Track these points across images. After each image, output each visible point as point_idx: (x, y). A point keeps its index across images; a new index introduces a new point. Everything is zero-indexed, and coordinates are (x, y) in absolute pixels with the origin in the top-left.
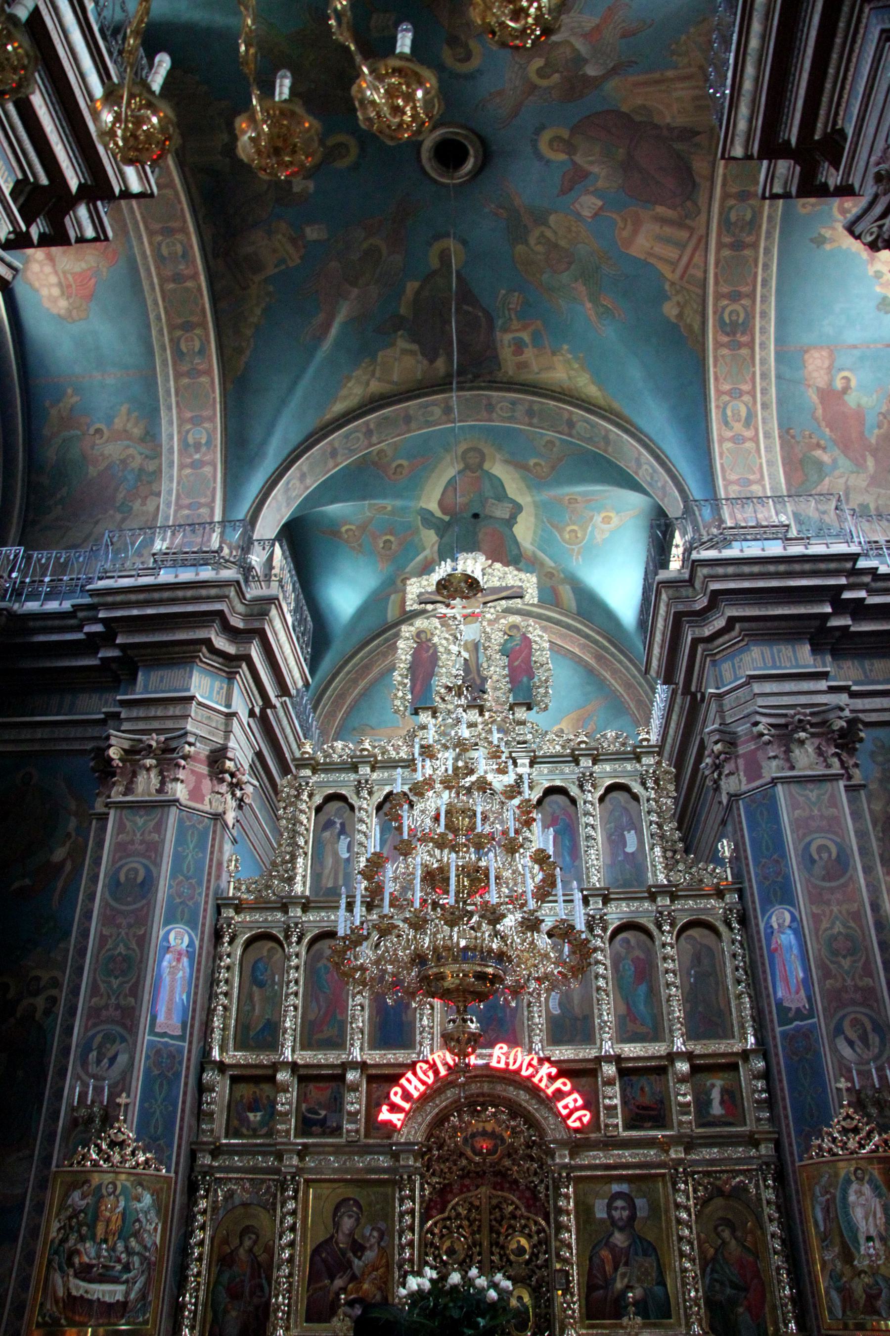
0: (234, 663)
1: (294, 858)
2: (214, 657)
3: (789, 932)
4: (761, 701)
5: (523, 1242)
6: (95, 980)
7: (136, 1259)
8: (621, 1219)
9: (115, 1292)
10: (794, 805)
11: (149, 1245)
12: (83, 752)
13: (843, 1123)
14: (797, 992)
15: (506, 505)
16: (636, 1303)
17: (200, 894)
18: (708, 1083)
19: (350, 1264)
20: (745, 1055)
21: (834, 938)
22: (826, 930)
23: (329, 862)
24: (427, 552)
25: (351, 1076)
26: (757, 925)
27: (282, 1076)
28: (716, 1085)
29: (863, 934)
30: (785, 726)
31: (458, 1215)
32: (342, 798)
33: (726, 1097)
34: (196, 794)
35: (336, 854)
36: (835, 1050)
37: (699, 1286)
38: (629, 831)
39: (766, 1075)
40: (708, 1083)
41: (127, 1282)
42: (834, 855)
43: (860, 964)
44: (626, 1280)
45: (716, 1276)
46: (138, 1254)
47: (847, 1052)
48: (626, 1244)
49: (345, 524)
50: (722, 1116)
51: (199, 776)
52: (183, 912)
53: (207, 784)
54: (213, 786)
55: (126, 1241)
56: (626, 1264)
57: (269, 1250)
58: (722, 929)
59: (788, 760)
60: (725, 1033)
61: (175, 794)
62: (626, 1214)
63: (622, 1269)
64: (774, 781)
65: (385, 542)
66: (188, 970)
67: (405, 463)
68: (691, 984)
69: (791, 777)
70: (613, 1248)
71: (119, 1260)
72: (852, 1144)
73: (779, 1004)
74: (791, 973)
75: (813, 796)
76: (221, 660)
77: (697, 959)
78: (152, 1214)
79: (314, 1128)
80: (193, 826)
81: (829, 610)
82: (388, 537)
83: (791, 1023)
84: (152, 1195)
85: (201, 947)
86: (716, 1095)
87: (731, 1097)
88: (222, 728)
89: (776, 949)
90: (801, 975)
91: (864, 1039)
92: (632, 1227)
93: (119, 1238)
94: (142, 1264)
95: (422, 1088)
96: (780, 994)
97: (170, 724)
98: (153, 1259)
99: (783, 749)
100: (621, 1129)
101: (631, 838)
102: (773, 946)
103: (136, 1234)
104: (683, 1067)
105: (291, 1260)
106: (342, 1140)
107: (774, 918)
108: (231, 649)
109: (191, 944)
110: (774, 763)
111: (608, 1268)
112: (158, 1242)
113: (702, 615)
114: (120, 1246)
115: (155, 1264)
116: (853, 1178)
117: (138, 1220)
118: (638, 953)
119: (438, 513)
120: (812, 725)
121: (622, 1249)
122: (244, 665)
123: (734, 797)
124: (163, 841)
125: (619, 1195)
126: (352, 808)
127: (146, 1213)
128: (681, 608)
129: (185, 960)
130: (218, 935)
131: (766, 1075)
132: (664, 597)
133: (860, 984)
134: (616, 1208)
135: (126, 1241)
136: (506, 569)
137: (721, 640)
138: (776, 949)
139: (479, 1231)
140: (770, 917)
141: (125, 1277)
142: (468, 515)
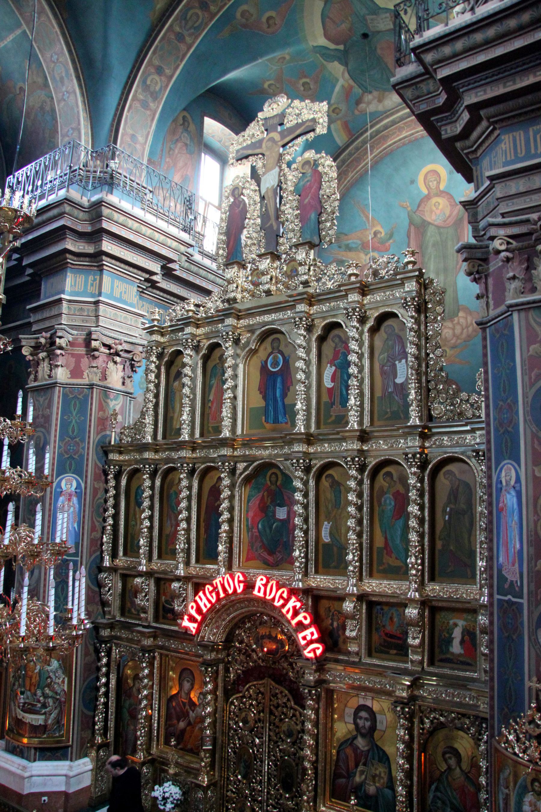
0: (98, 259)
2: (82, 259)
6: (24, 518)
7: (50, 701)
8: (364, 727)
9: (38, 719)
11: (59, 692)
15: (384, 16)
17: (83, 448)
18: (451, 622)
19: (188, 713)
24: (341, 82)
33: (466, 637)
38: (400, 362)
40: (451, 622)
41: (45, 714)
44: (363, 777)
45: (439, 794)
46: (51, 697)
48: (366, 748)
49: (264, 82)
50: (460, 655)
52: (71, 465)
54: (90, 362)
55: (43, 689)
56: (365, 764)
61: (56, 378)
62: (368, 724)
63: (361, 768)
65: (304, 84)
66: (77, 506)
67: (273, 14)
68: (445, 521)
69: (528, 303)
71: (39, 701)
76: (87, 259)
78: (60, 672)
79: (169, 615)
80: (75, 397)
82: (304, 80)
83: (506, 596)
84: (58, 661)
85: (86, 488)
88: (93, 314)
92: (372, 736)
93: (38, 688)
94: (54, 703)
95: (209, 605)
96: (501, 559)
97: (47, 324)
98: (63, 699)
99: (524, 266)
102: (501, 505)
103: (49, 686)
108: (90, 249)
109: (79, 486)
110: (514, 285)
111: (352, 764)
112: (66, 689)
114: (39, 692)
115: (65, 702)
117: (50, 677)
119: (332, 46)
121: (362, 751)
122: (104, 258)
124: (52, 414)
127: (55, 673)
129: (75, 499)
134: (361, 718)
135: (43, 689)
136: (303, 104)
139: (263, 711)
141: (43, 711)
142: (357, 37)
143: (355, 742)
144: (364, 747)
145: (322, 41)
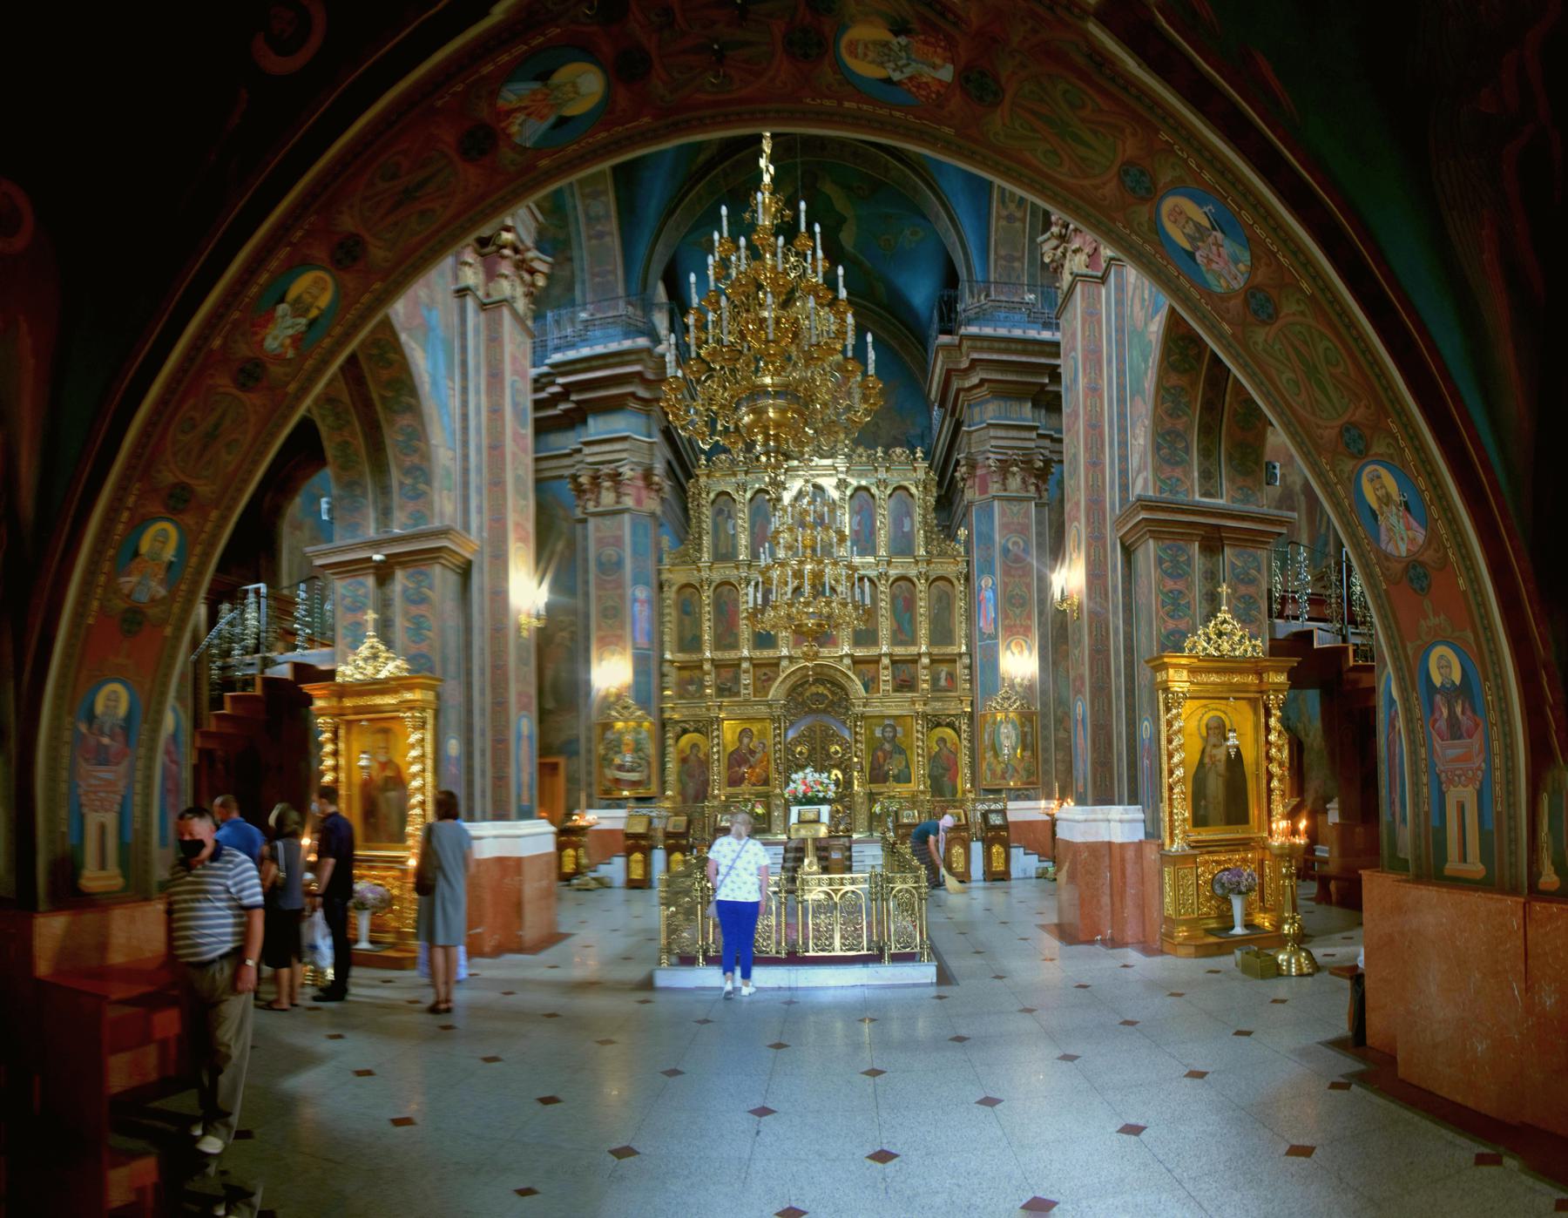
1: (700, 538)
4: (994, 443)
10: (1003, 514)
12: (561, 477)
16: (894, 776)
19: (749, 761)
20: (960, 655)
23: (722, 536)
25: (745, 665)
27: (707, 667)
28: (944, 670)
30: (1006, 461)
32: (728, 494)
34: (639, 501)
35: (726, 532)
37: (927, 768)
39: (970, 667)
51: (638, 488)
53: (644, 493)
57: (707, 755)
58: (956, 582)
59: (1004, 484)
60: (952, 643)
64: (994, 497)
70: (884, 751)
72: (1006, 705)
73: (980, 629)
75: (1015, 509)
77: (940, 599)
81: (1047, 381)
86: (943, 675)
87: (951, 677)
101: (907, 522)
104: (925, 661)
105: (718, 760)
106: (741, 699)
111: (881, 760)
113: (966, 372)
118: (906, 594)
120: (1022, 462)
123: (971, 503)
126: (734, 500)
128: (951, 366)
130: (661, 586)
131: (970, 667)
132: (940, 355)
137: (975, 391)
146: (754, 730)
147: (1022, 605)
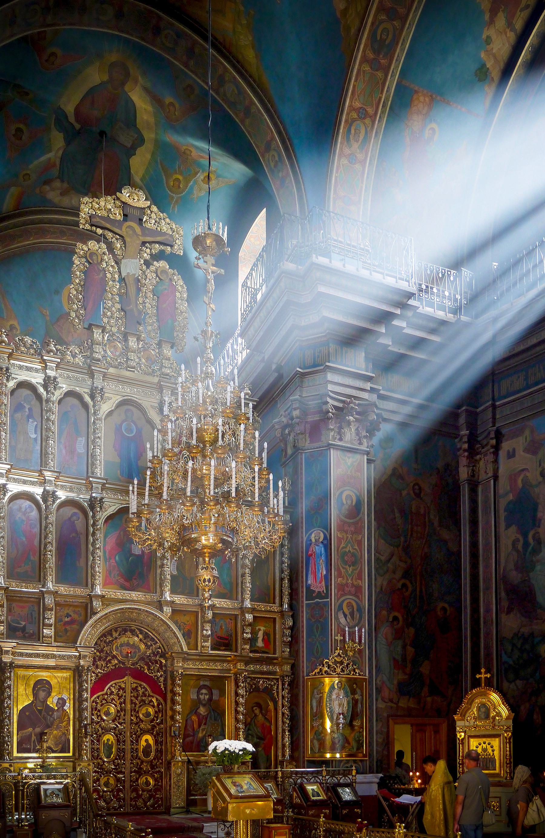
3: (321, 545)
5: (151, 710)
13: (335, 658)
14: (320, 582)
21: (345, 554)
22: (343, 548)
26: (302, 538)
29: (361, 554)
31: (112, 693)
36: (337, 619)
42: (354, 503)
43: (357, 571)
44: (204, 732)
47: (343, 620)
56: (205, 724)
62: (207, 697)
63: (203, 727)
73: (308, 587)
74: (319, 570)
86: (260, 635)
89: (312, 555)
90: (324, 573)
91: (352, 614)
100: (210, 649)
107: (313, 535)
116: (336, 687)
125: (204, 687)
133: (355, 583)
134: (202, 694)
138: (312, 555)
140: (311, 534)
143: (198, 711)
144: (204, 713)
145: (70, 109)
146: (53, 682)
147: (353, 564)
